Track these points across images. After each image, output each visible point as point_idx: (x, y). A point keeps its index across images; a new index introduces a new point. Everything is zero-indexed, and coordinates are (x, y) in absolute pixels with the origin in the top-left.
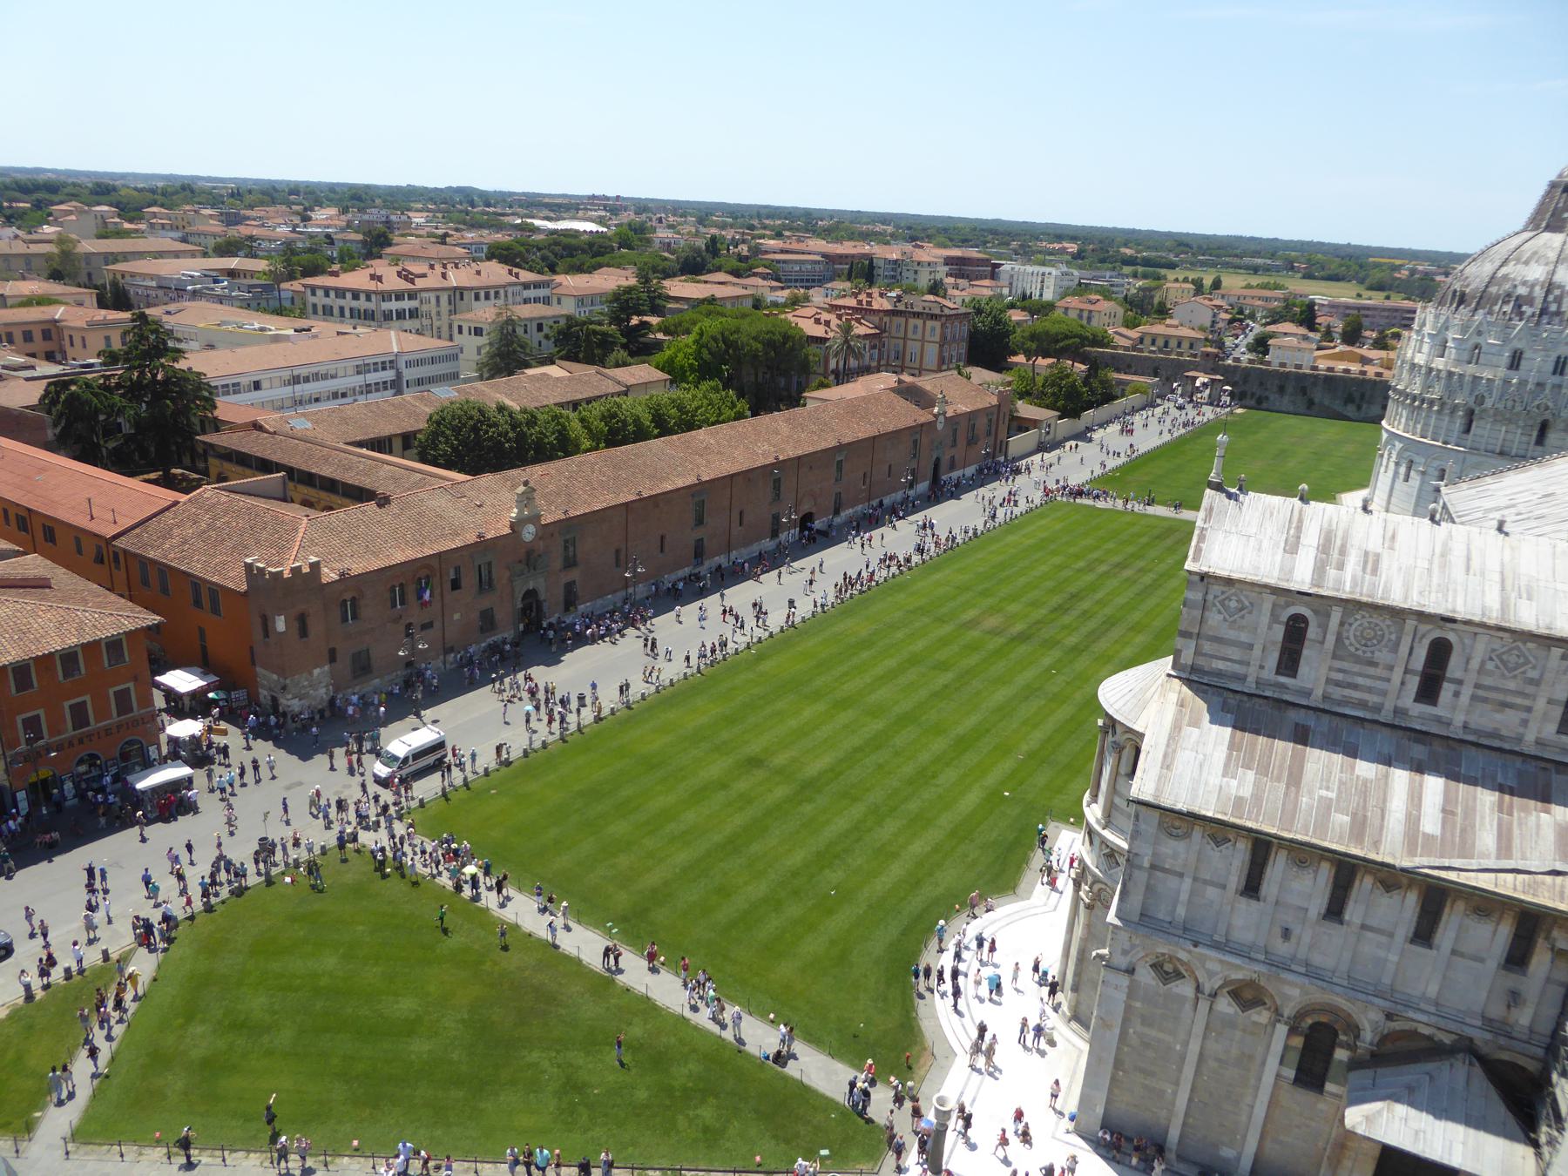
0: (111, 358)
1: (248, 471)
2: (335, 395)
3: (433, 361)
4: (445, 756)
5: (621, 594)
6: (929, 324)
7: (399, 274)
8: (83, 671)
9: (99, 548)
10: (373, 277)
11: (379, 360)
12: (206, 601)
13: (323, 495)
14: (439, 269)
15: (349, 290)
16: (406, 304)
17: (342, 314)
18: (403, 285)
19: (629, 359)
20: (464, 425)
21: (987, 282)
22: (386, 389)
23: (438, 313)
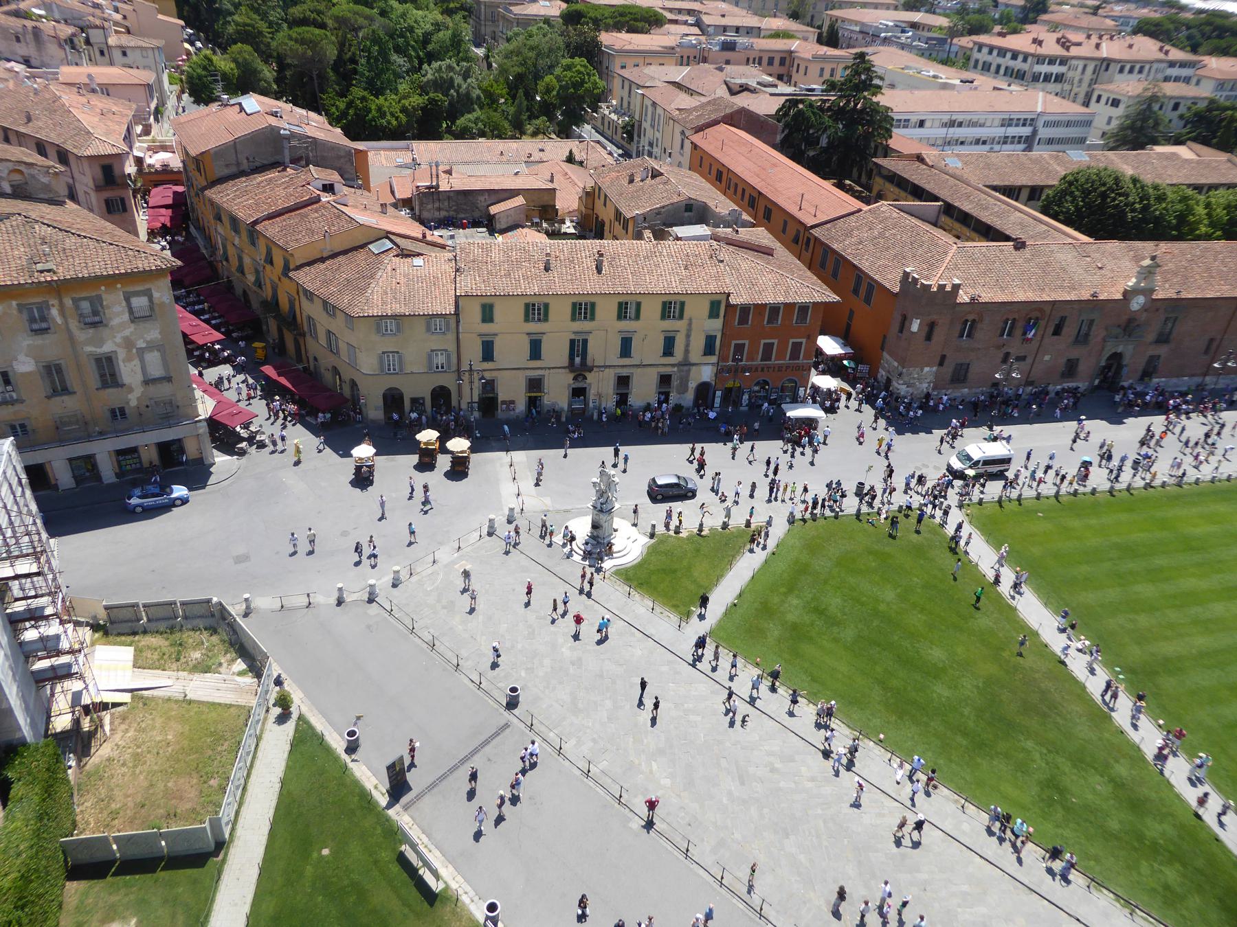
0: (832, 86)
1: (903, 194)
2: (977, 142)
3: (1068, 124)
4: (1007, 470)
5: (1198, 380)
9: (798, 231)
10: (1035, 41)
11: (1023, 117)
13: (957, 226)
14: (1094, 39)
15: (1010, 50)
16: (1056, 69)
17: (997, 72)
18: (1058, 51)
20: (1095, 190)
22: (1019, 142)
23: (1080, 81)
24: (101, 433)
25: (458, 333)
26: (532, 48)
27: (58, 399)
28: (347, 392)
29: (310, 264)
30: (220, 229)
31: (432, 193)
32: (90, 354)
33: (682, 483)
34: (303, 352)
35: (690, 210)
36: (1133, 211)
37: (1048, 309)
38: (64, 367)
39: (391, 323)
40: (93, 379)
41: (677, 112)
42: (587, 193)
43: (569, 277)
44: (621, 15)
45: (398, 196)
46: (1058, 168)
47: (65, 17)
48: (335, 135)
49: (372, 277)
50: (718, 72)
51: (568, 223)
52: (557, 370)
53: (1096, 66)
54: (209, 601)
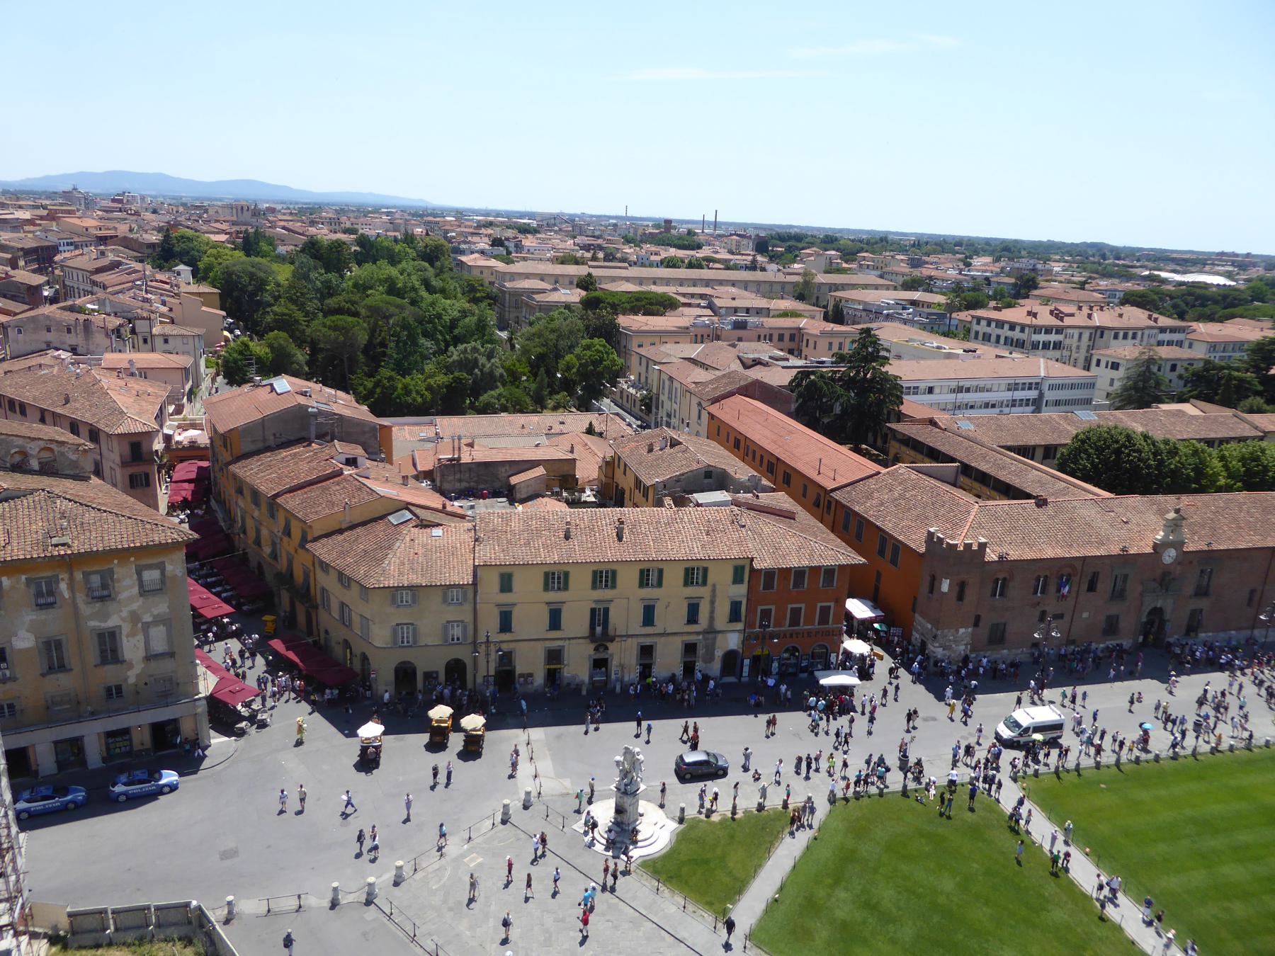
0: (841, 358)
1: (919, 457)
2: (987, 405)
3: (1072, 386)
4: (1060, 737)
5: (1246, 633)
7: (1051, 313)
8: (806, 586)
9: (819, 495)
10: (1029, 313)
11: (1027, 381)
13: (976, 485)
14: (1086, 310)
16: (1053, 338)
17: (998, 341)
18: (1054, 322)
19: (1265, 407)
20: (1108, 447)
22: (1027, 405)
23: (1078, 347)
24: (93, 714)
25: (475, 604)
26: (553, 331)
27: (52, 676)
28: (357, 666)
29: (327, 535)
30: (241, 503)
31: (454, 466)
32: (94, 629)
33: (712, 760)
34: (314, 623)
35: (710, 478)
36: (1149, 467)
37: (1079, 565)
38: (64, 642)
39: (407, 594)
40: (92, 654)
41: (694, 385)
42: (607, 463)
43: (590, 545)
44: (637, 300)
45: (419, 469)
46: (1069, 428)
47: (115, 310)
48: (362, 412)
49: (389, 548)
50: (731, 348)
51: (588, 492)
52: (581, 641)
53: (1091, 334)
54: (187, 905)
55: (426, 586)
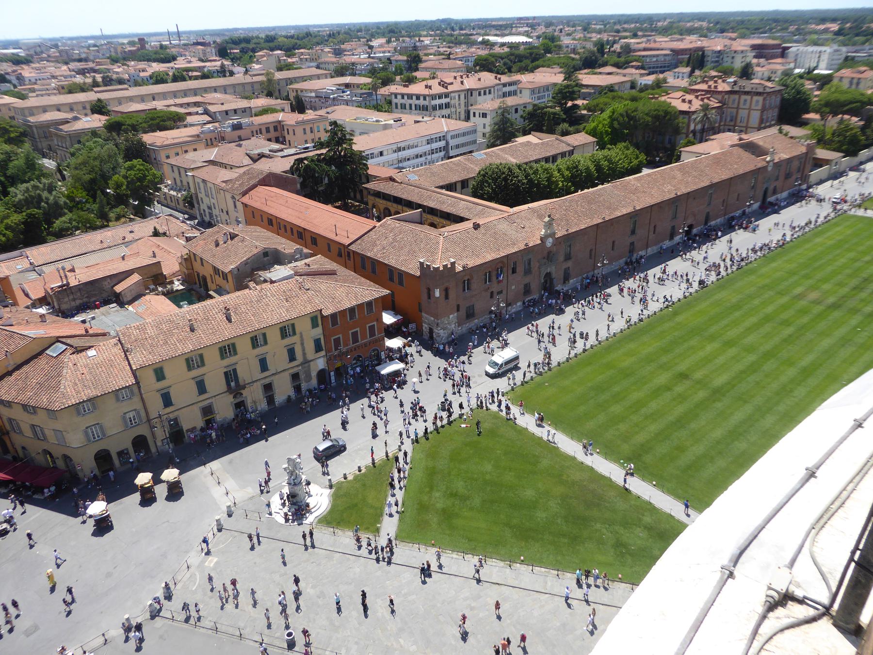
0: (320, 145)
2: (417, 157)
3: (464, 134)
6: (755, 98)
10: (426, 87)
11: (438, 136)
12: (396, 278)
14: (459, 79)
15: (414, 95)
16: (444, 101)
17: (411, 108)
21: (779, 60)
22: (440, 151)
23: (459, 104)
25: (141, 394)
26: (95, 159)
31: (65, 290)
33: (336, 443)
36: (523, 184)
37: (505, 260)
41: (224, 184)
42: (186, 259)
43: (211, 331)
44: (152, 119)
45: (33, 297)
49: (59, 375)
50: (238, 148)
51: (177, 283)
55: (102, 395)
